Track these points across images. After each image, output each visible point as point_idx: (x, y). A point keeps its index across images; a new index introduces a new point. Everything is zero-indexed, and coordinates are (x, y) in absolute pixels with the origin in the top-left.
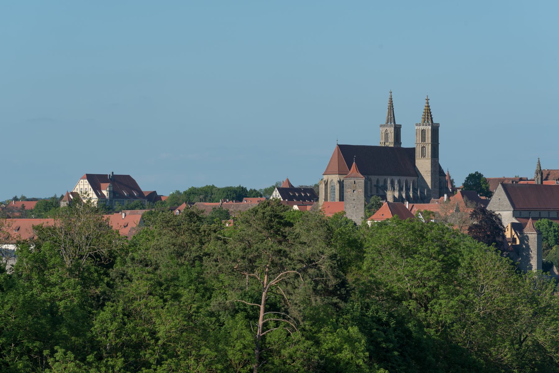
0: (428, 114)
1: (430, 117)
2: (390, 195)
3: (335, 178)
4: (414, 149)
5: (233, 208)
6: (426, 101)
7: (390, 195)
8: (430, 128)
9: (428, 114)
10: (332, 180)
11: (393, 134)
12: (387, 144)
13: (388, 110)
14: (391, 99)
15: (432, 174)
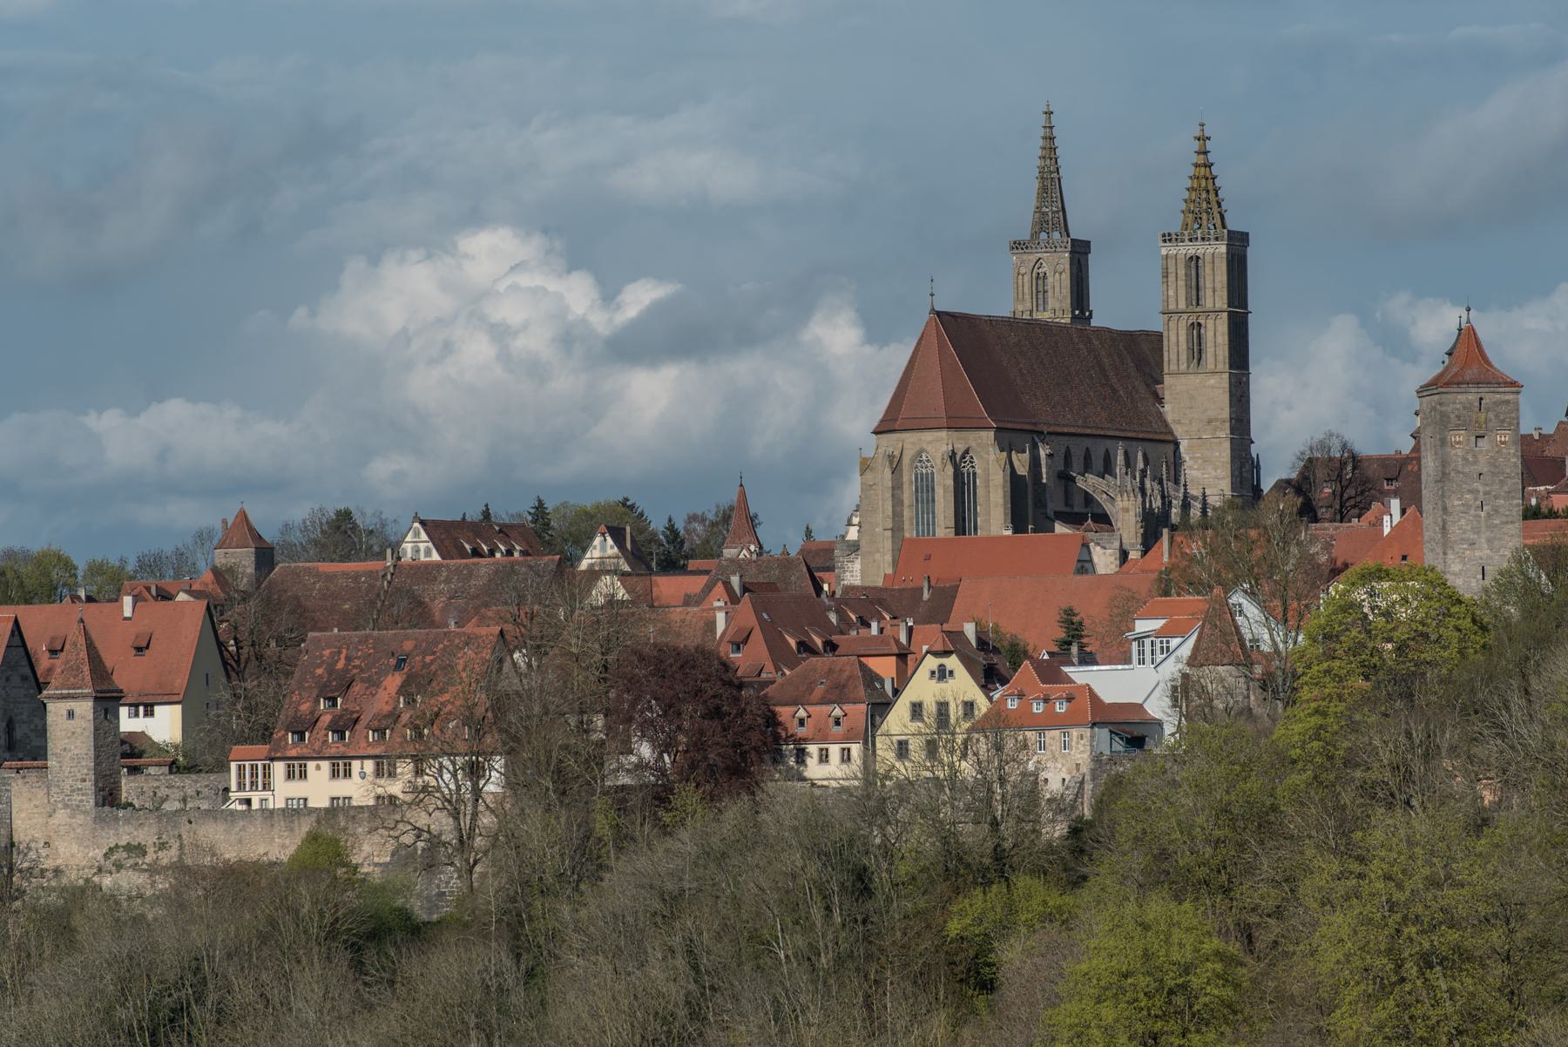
0: (1205, 200)
1: (1215, 209)
2: (1126, 510)
3: (936, 445)
4: (1156, 339)
5: (448, 581)
6: (1196, 145)
7: (1126, 510)
8: (1223, 249)
9: (1205, 200)
10: (919, 454)
11: (1066, 277)
12: (1038, 316)
13: (1035, 185)
14: (1052, 139)
15: (1232, 431)
